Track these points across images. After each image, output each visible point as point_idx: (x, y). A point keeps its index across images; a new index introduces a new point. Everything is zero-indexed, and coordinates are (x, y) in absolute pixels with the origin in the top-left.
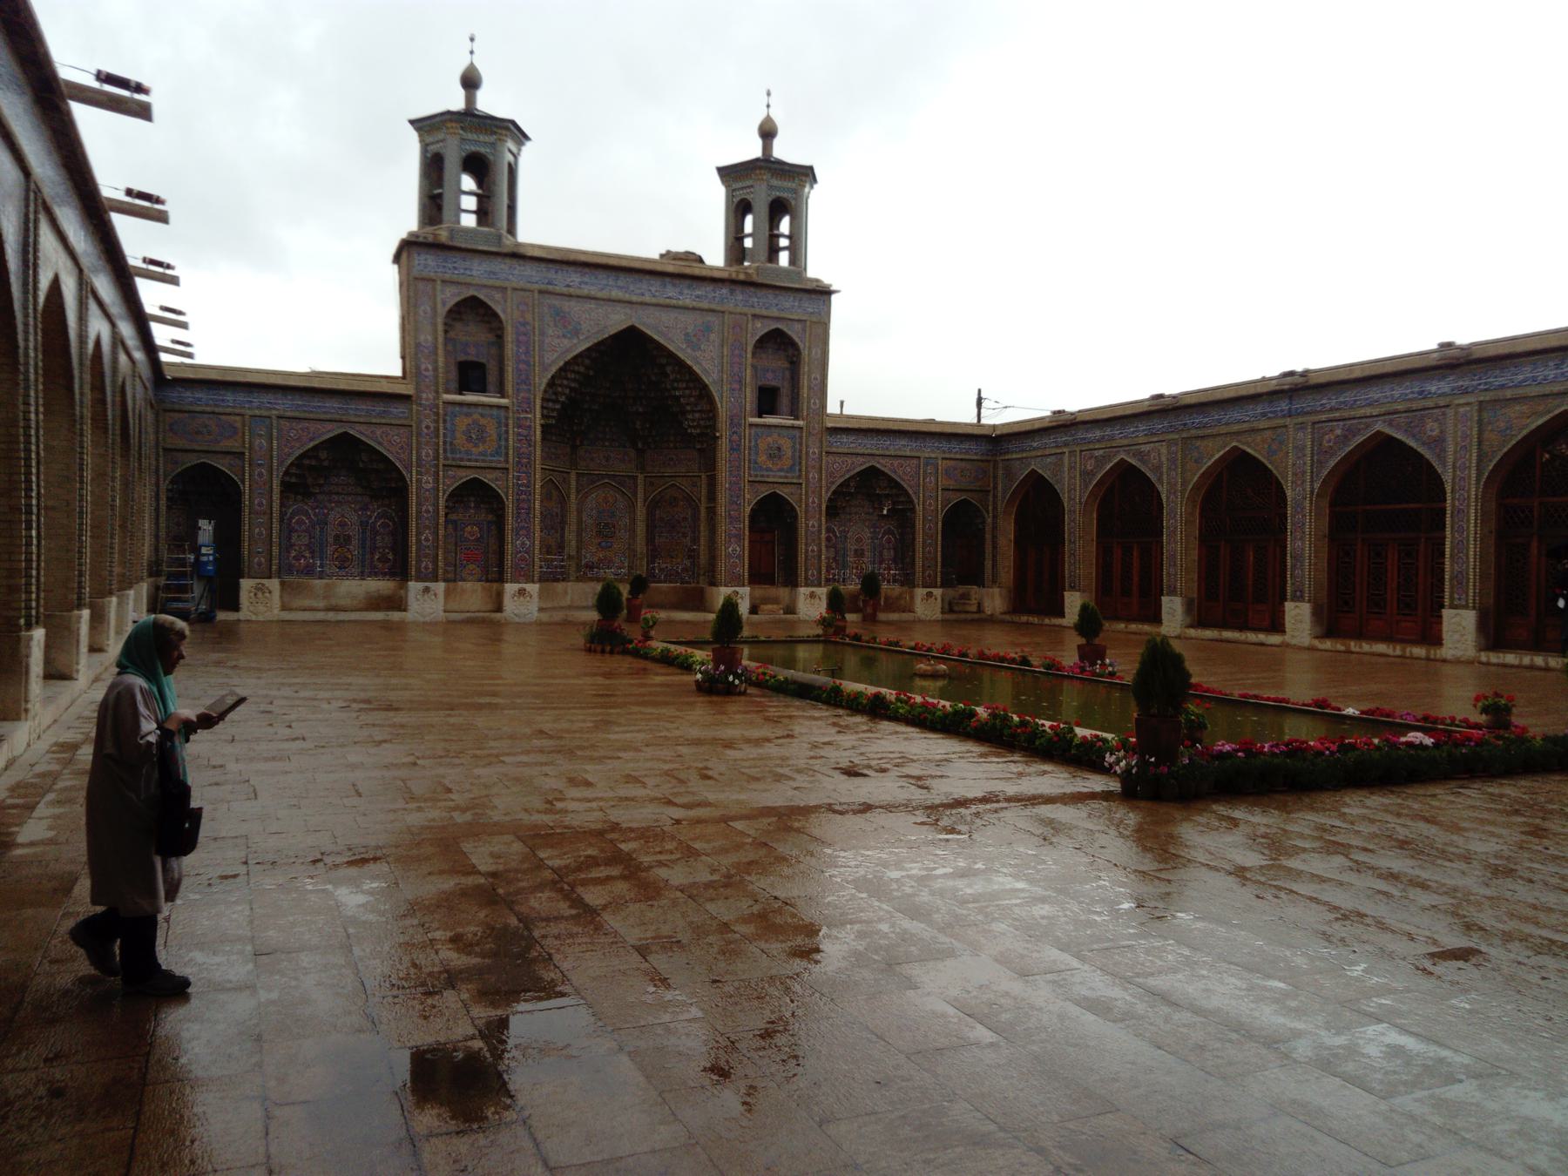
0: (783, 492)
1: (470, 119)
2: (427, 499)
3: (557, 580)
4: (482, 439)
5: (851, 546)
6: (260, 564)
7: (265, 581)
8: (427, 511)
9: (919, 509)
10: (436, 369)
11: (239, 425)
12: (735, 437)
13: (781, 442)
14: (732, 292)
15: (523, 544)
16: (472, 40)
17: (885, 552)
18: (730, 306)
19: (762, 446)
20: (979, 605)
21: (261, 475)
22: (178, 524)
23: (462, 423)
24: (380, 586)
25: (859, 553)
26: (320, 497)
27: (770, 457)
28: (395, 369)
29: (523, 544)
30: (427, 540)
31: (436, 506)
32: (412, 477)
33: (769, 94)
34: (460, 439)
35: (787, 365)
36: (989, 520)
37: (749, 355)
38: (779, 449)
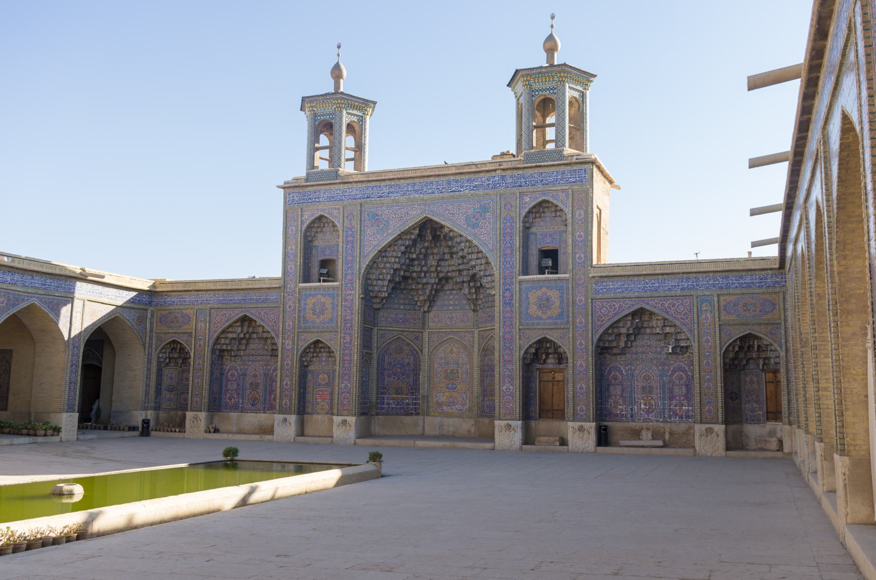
0: (552, 336)
1: (340, 99)
2: (287, 357)
3: (408, 414)
4: (322, 312)
5: (639, 384)
6: (197, 402)
7: (199, 413)
8: (287, 364)
9: (695, 345)
10: (296, 266)
11: (191, 315)
12: (507, 294)
13: (549, 293)
14: (503, 177)
15: (346, 386)
16: (339, 47)
17: (676, 390)
18: (502, 190)
19: (533, 297)
20: (781, 442)
21: (200, 345)
22: (171, 378)
23: (311, 301)
24: (262, 418)
25: (647, 390)
26: (243, 358)
27: (540, 307)
28: (276, 272)
29: (346, 386)
30: (287, 384)
31: (292, 360)
32: (279, 342)
33: (553, 17)
34: (309, 315)
35: (563, 228)
36: (783, 354)
37: (518, 226)
38: (548, 300)
